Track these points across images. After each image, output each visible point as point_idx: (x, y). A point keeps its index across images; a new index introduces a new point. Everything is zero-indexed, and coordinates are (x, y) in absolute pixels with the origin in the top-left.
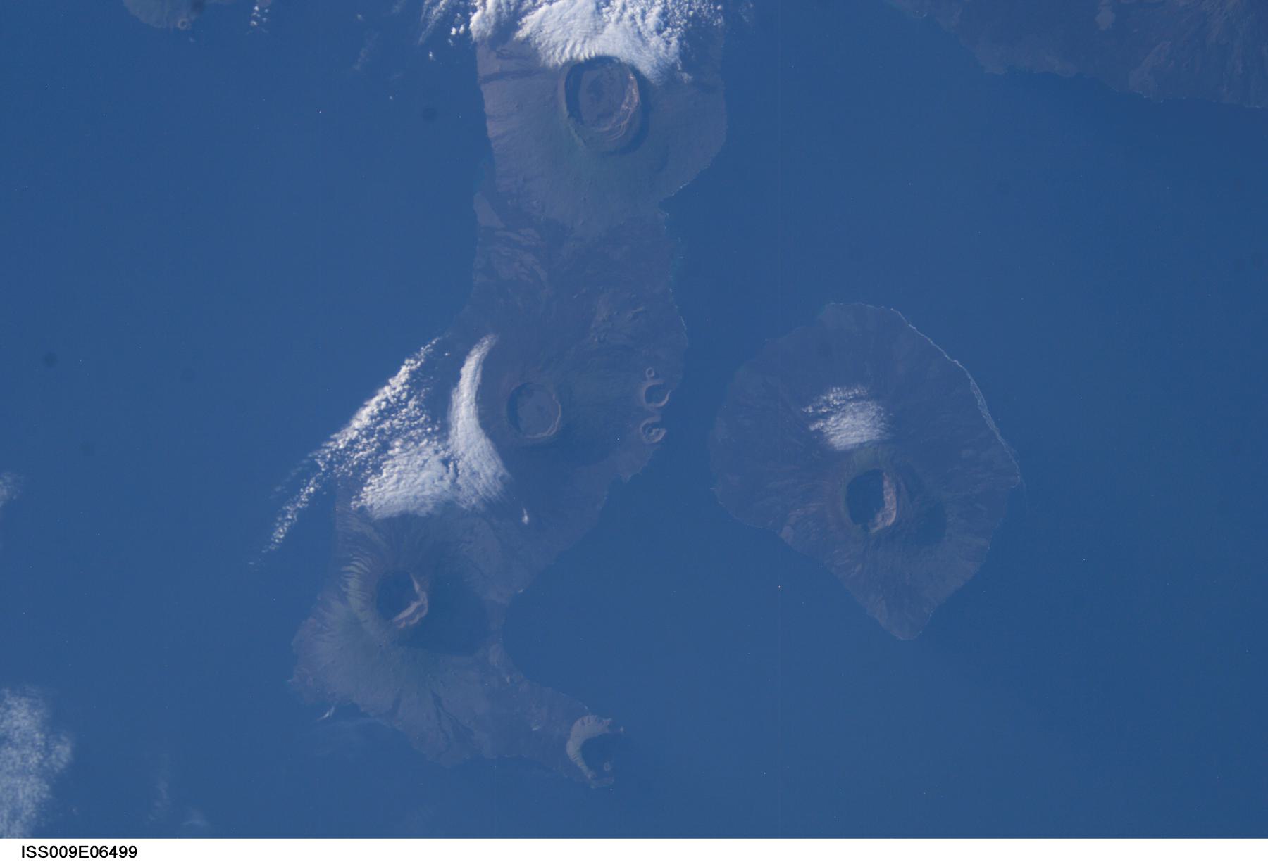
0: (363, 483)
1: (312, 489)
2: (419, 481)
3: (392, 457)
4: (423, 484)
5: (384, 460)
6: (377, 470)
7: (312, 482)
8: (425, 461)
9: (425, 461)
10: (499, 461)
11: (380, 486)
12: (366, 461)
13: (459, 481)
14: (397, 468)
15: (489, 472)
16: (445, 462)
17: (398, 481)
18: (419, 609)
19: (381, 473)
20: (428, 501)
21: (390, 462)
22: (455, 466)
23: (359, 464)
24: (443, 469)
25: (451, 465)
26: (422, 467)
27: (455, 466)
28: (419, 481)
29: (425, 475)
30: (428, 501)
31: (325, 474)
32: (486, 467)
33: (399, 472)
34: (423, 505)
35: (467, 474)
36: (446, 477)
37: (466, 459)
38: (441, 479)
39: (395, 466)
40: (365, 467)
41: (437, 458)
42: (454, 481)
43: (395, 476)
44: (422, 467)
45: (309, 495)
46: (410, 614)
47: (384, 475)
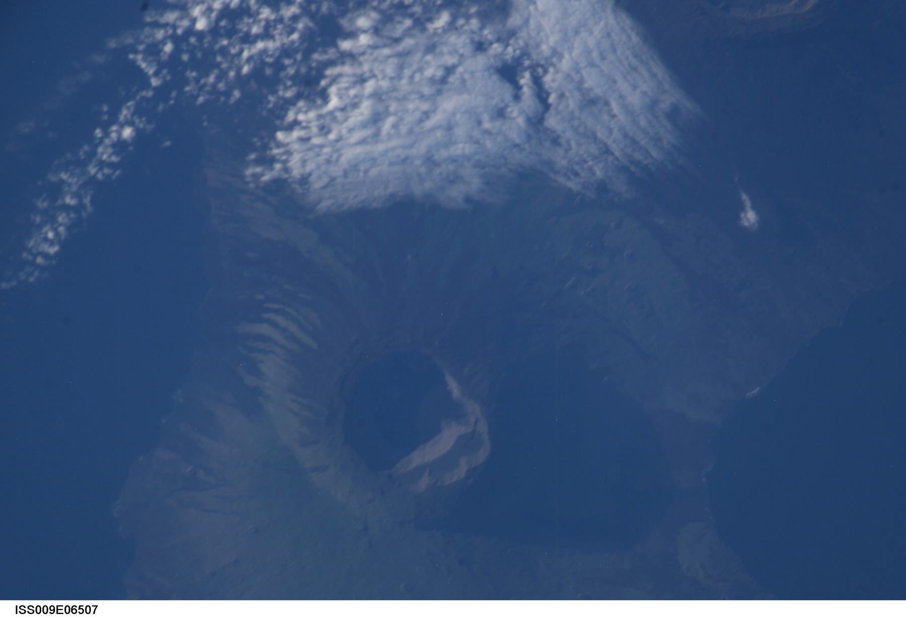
0: (275, 120)
1: (127, 132)
2: (436, 119)
3: (351, 57)
4: (449, 128)
5: (331, 63)
6: (311, 87)
7: (125, 113)
8: (450, 70)
9: (450, 70)
10: (660, 71)
11: (324, 130)
12: (278, 66)
13: (552, 121)
14: (370, 86)
15: (635, 99)
16: (508, 72)
17: (376, 119)
18: (467, 443)
19: (324, 97)
20: (468, 171)
21: (347, 69)
22: (537, 81)
23: (257, 73)
24: (507, 91)
25: (525, 80)
26: (441, 83)
27: (537, 81)
28: (436, 119)
29: (449, 104)
30: (468, 171)
31: (162, 93)
32: (624, 87)
33: (377, 96)
34: (454, 179)
35: (572, 103)
36: (514, 111)
37: (565, 64)
38: (501, 114)
39: (361, 80)
40: (272, 84)
41: (481, 61)
42: (536, 122)
43: (366, 108)
44: (441, 83)
45: (120, 146)
46: (446, 451)
47: (334, 102)
